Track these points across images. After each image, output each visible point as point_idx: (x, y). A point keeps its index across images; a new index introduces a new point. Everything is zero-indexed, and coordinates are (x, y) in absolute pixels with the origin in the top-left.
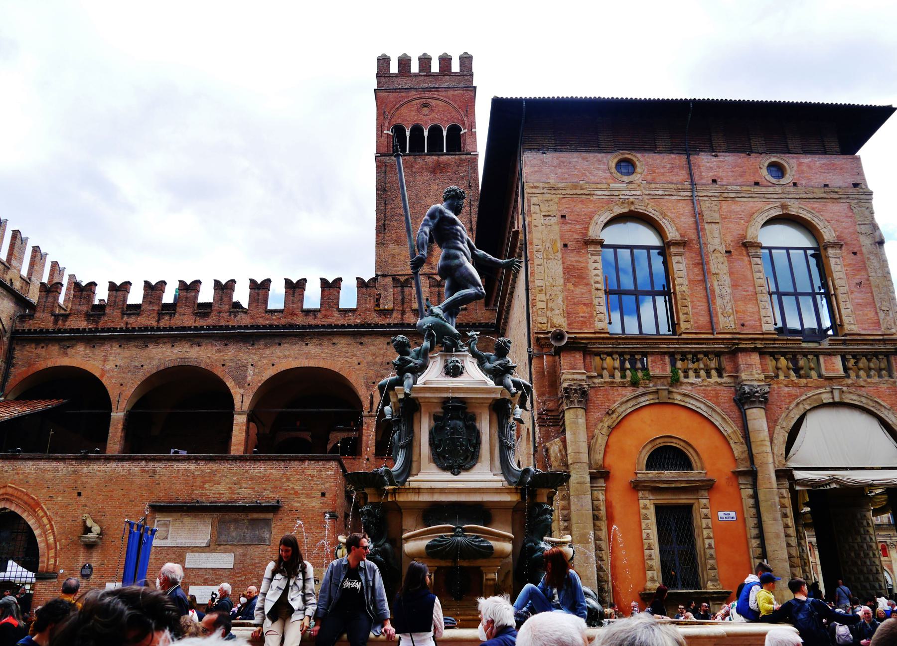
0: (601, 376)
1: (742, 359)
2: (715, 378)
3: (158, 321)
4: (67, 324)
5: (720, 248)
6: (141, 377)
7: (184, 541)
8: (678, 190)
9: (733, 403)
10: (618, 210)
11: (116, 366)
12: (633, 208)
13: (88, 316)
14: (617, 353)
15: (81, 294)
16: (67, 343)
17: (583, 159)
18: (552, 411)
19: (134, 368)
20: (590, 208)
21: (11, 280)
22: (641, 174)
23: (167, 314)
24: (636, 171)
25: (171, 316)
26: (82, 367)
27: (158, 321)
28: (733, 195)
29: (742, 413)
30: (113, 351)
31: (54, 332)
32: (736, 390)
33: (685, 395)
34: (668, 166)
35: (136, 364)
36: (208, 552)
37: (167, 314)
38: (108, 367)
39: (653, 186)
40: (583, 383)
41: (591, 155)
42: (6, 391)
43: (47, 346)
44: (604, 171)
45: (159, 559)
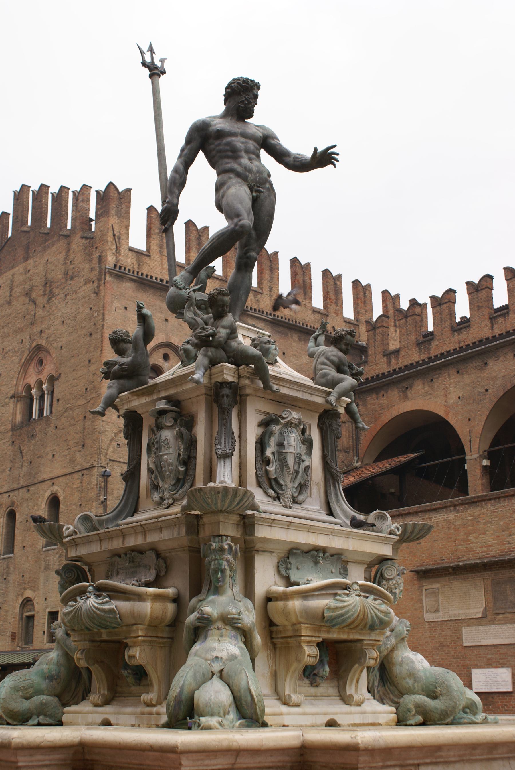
3: (492, 329)
4: (400, 361)
6: (488, 404)
7: (457, 612)
11: (459, 398)
13: (419, 344)
15: (406, 322)
16: (405, 384)
19: (478, 395)
23: (500, 315)
25: (505, 317)
26: (425, 409)
27: (492, 328)
30: (452, 381)
31: (390, 374)
35: (480, 390)
36: (486, 624)
37: (500, 315)
38: (451, 402)
42: (361, 455)
43: (387, 393)
45: (434, 637)
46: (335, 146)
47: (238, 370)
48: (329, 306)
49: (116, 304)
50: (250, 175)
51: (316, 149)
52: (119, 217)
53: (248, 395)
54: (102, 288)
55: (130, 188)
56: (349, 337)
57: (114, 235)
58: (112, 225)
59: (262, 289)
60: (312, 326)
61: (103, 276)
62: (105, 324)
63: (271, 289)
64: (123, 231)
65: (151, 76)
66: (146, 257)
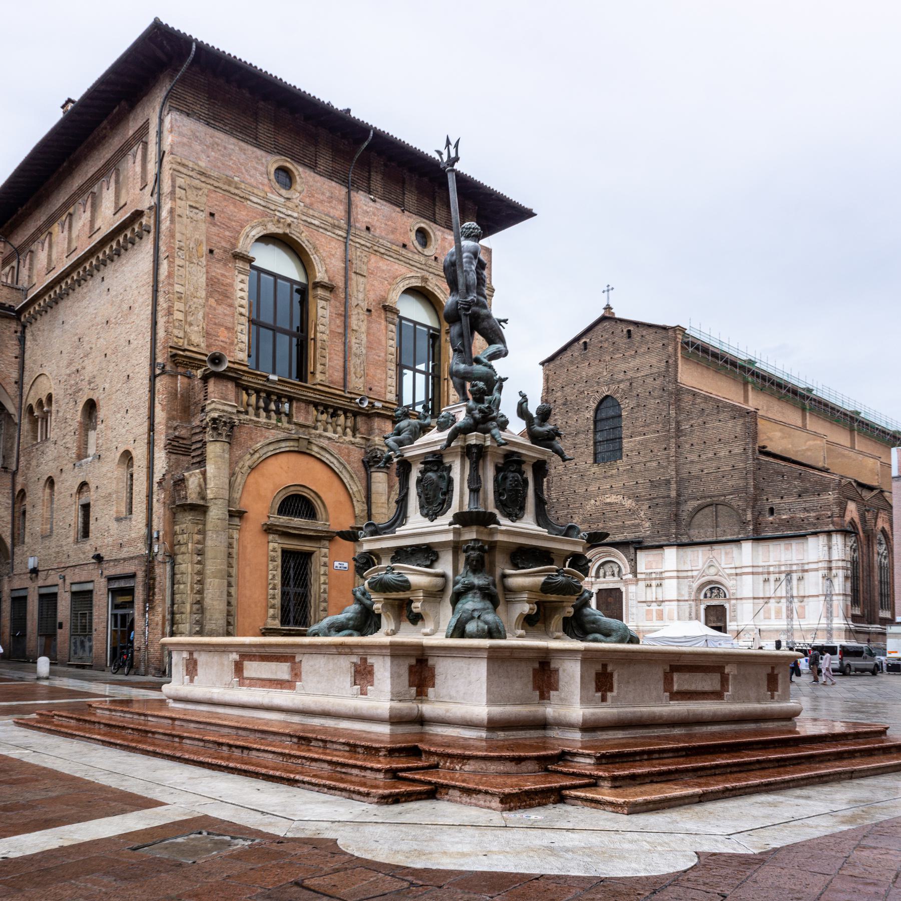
0: (247, 413)
1: (377, 423)
2: (349, 438)
5: (362, 304)
8: (334, 226)
9: (361, 464)
10: (272, 229)
12: (288, 231)
14: (265, 391)
17: (241, 149)
18: (184, 439)
20: (243, 215)
22: (300, 193)
24: (293, 187)
28: (383, 251)
29: (367, 474)
32: (366, 453)
33: (322, 448)
34: (328, 194)
39: (311, 212)
40: (233, 417)
41: (250, 147)
44: (261, 174)
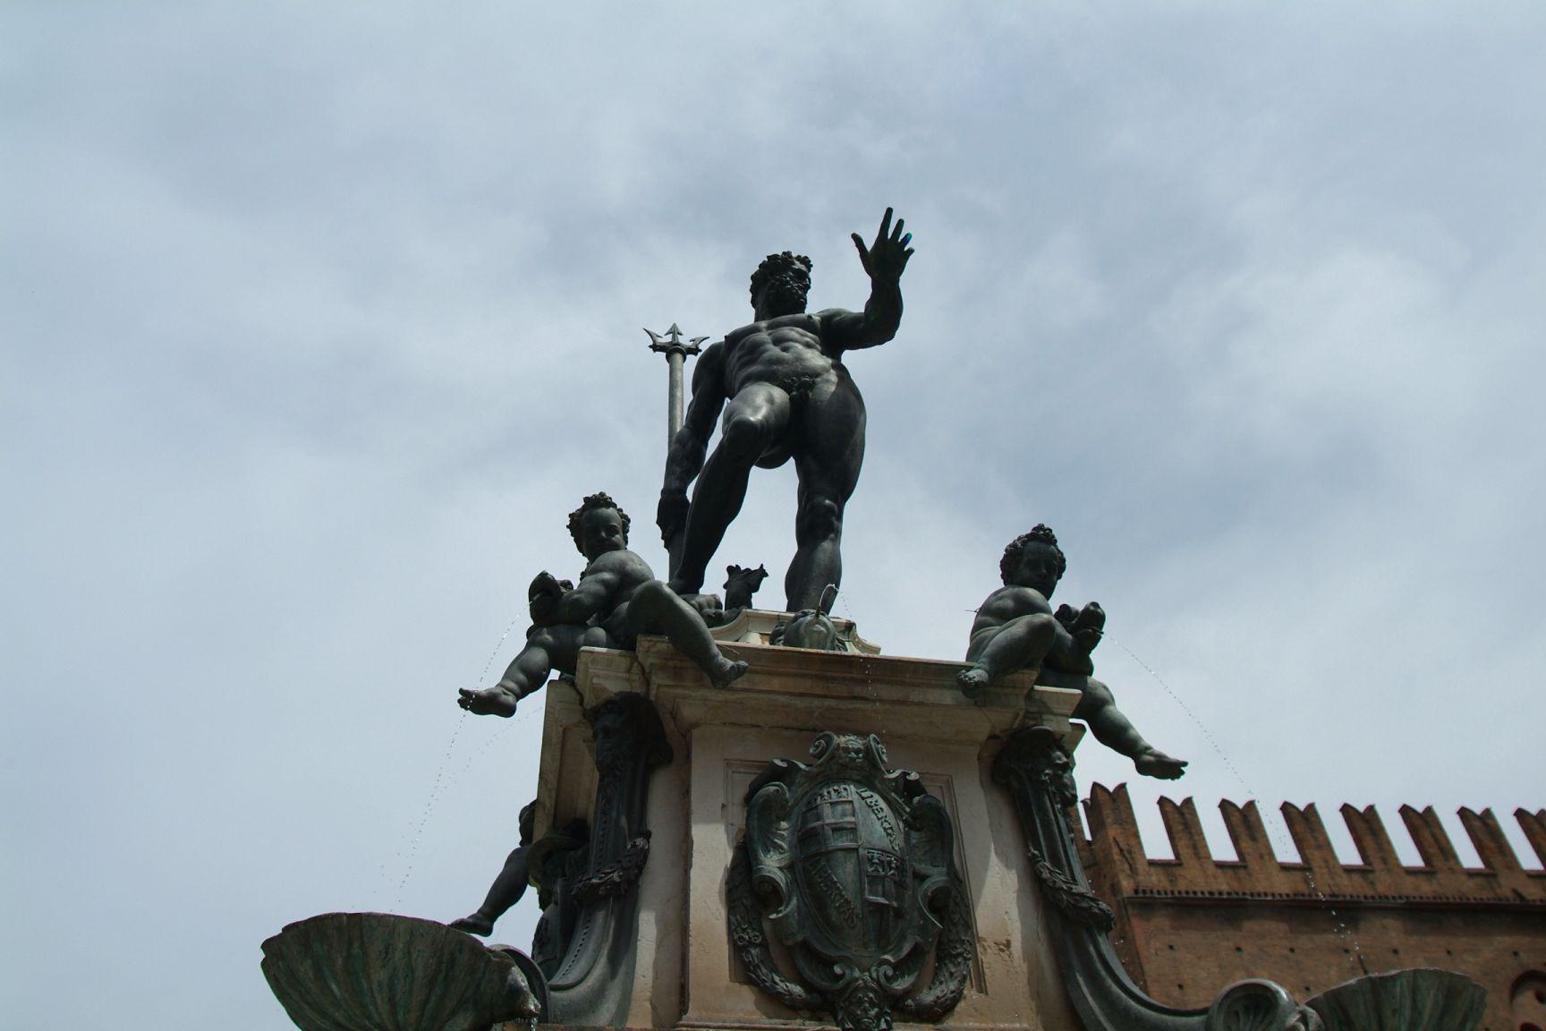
21: (1514, 891)
46: (889, 211)
47: (635, 658)
48: (1491, 860)
49: (1155, 944)
50: (780, 368)
51: (858, 240)
52: (1121, 824)
53: (696, 725)
54: (1127, 928)
55: (1124, 782)
56: (1032, 544)
57: (1121, 850)
58: (1114, 839)
59: (1370, 864)
60: (1478, 896)
61: (1124, 912)
62: (1147, 978)
63: (1384, 861)
64: (1132, 841)
65: (668, 358)
66: (1178, 868)
